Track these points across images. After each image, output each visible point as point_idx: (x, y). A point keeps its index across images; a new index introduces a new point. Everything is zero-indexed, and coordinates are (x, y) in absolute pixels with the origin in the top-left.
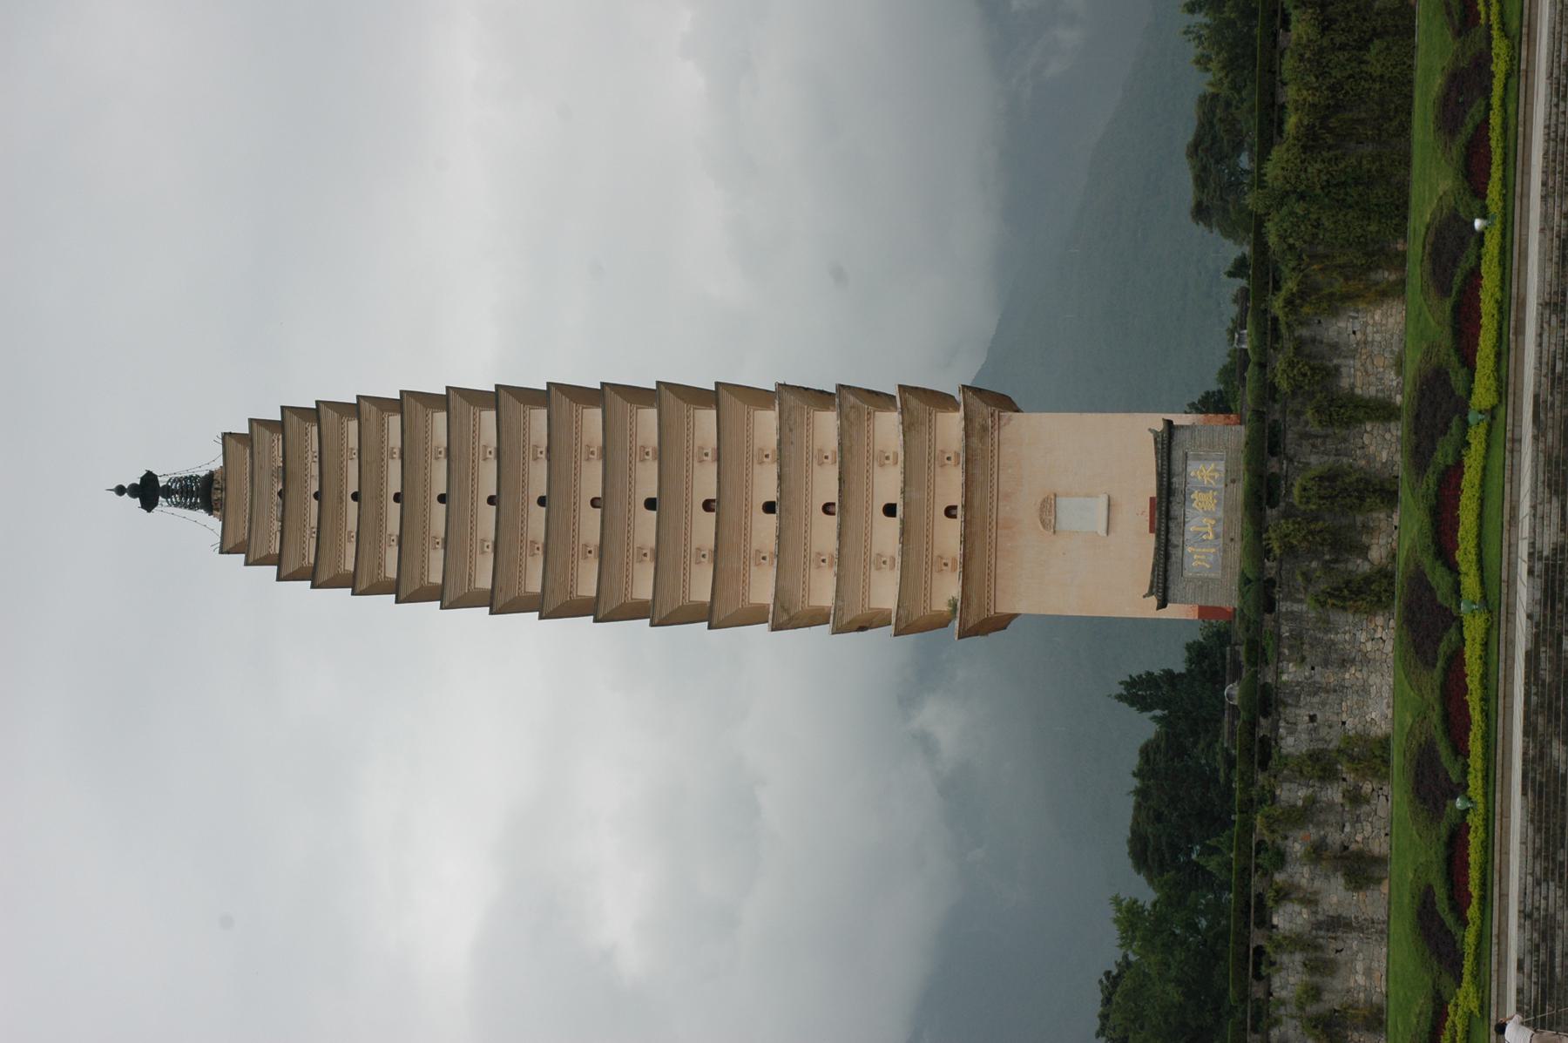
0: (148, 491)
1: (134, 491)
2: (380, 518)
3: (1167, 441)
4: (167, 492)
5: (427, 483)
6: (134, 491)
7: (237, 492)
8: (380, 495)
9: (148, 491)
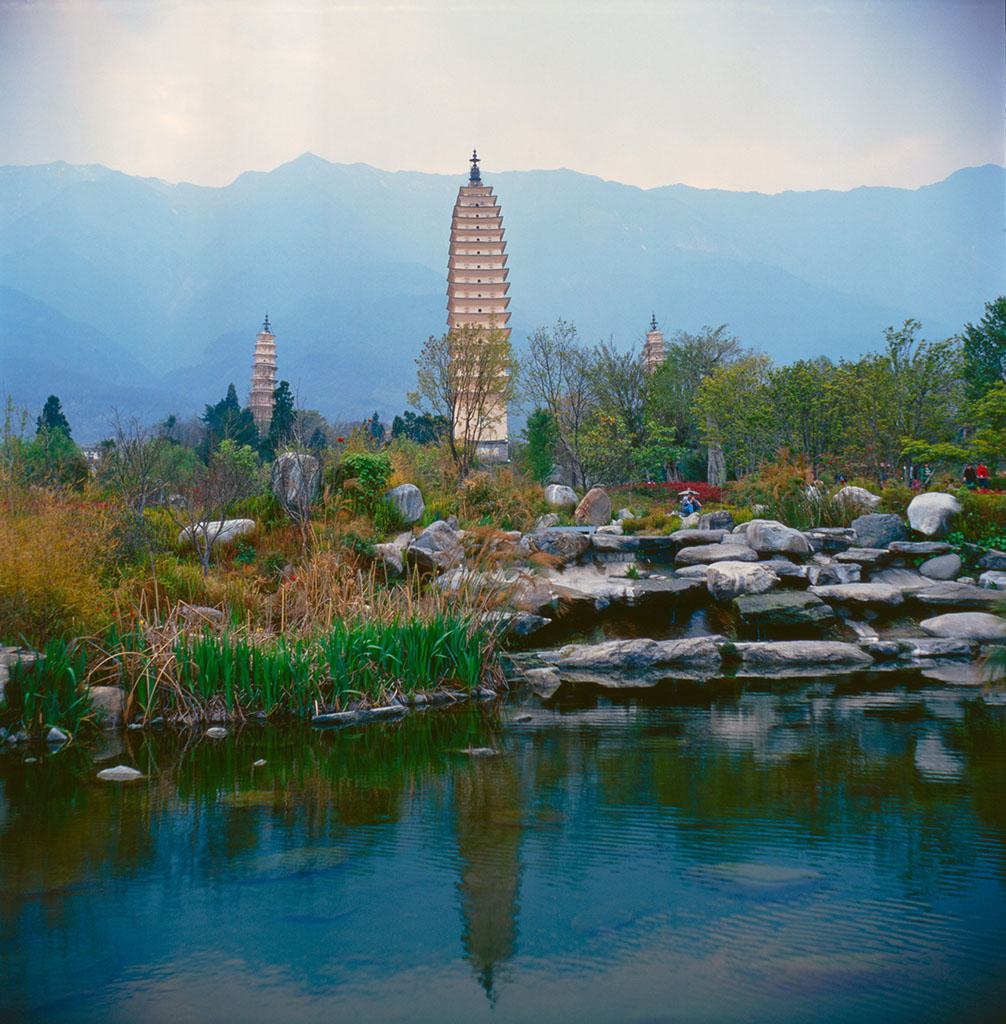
0: (475, 160)
1: (475, 156)
2: (472, 235)
3: (502, 442)
4: (475, 165)
5: (482, 249)
6: (475, 156)
7: (476, 191)
8: (479, 235)
9: (475, 160)
